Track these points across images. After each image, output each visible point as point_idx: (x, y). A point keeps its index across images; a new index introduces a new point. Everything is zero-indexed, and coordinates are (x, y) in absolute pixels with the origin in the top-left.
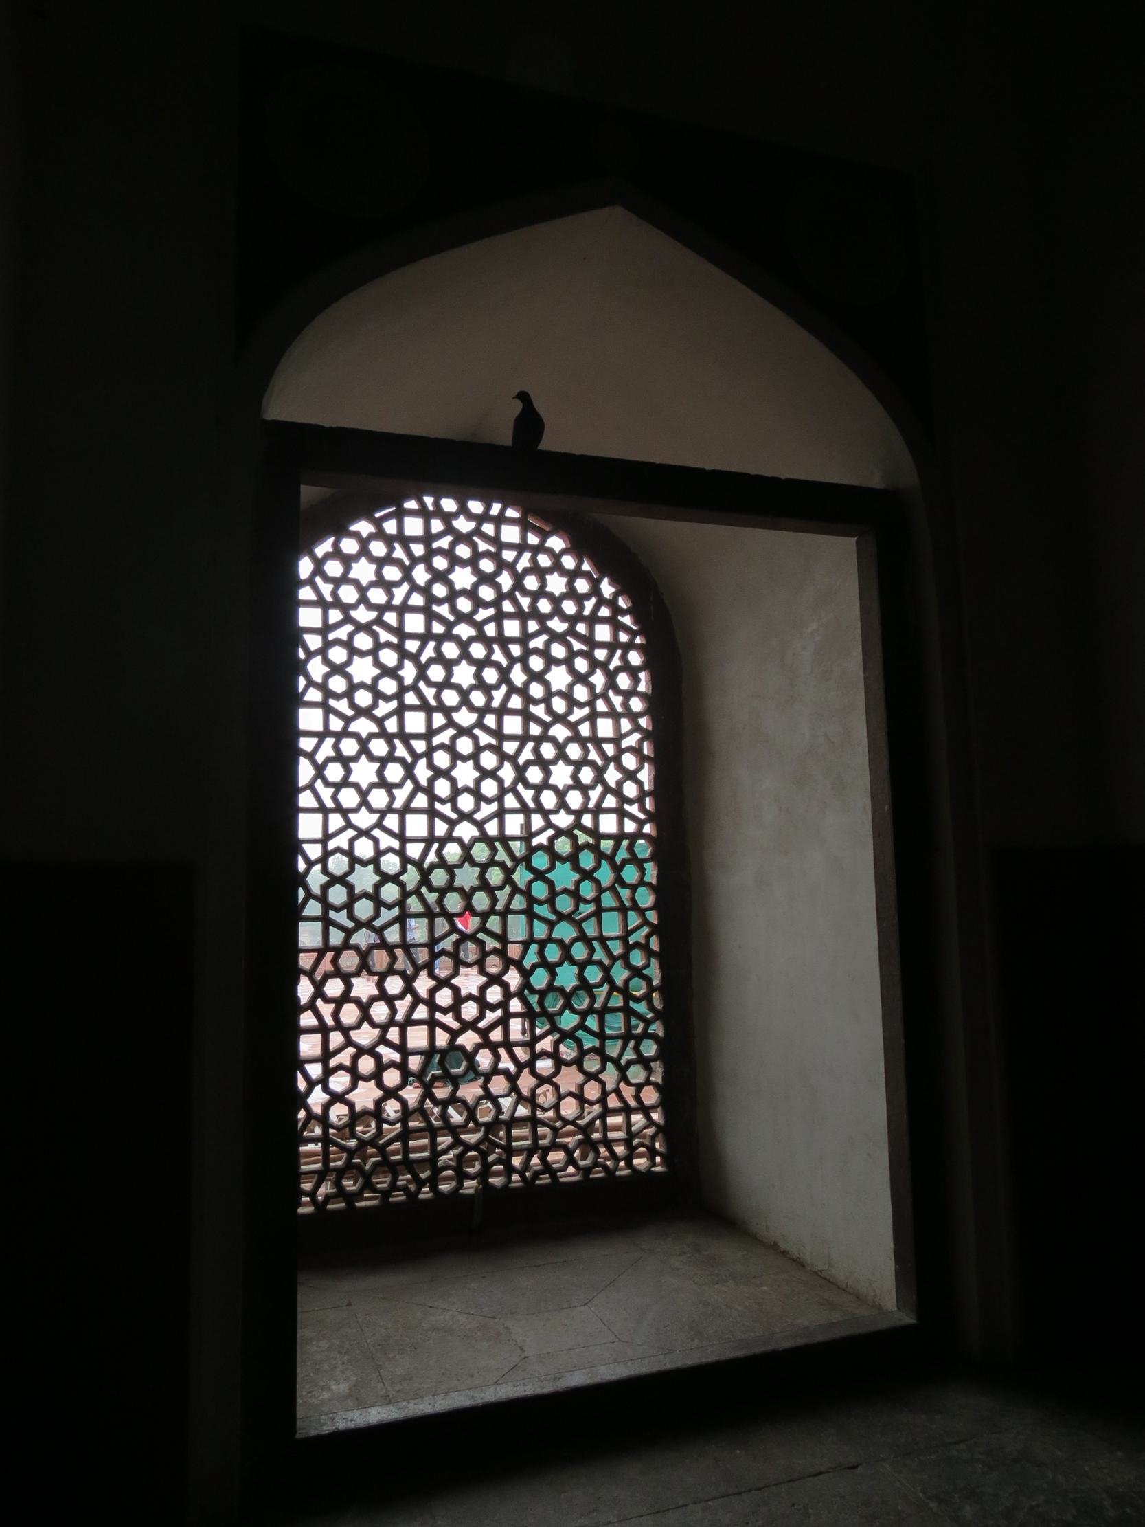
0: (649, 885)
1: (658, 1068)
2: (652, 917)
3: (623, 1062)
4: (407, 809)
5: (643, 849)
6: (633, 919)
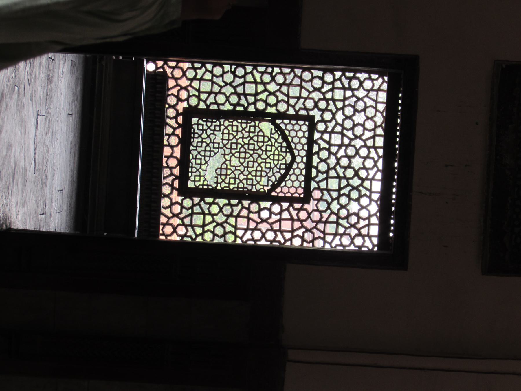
1: (222, 240)
4: (343, 135)
6: (288, 236)
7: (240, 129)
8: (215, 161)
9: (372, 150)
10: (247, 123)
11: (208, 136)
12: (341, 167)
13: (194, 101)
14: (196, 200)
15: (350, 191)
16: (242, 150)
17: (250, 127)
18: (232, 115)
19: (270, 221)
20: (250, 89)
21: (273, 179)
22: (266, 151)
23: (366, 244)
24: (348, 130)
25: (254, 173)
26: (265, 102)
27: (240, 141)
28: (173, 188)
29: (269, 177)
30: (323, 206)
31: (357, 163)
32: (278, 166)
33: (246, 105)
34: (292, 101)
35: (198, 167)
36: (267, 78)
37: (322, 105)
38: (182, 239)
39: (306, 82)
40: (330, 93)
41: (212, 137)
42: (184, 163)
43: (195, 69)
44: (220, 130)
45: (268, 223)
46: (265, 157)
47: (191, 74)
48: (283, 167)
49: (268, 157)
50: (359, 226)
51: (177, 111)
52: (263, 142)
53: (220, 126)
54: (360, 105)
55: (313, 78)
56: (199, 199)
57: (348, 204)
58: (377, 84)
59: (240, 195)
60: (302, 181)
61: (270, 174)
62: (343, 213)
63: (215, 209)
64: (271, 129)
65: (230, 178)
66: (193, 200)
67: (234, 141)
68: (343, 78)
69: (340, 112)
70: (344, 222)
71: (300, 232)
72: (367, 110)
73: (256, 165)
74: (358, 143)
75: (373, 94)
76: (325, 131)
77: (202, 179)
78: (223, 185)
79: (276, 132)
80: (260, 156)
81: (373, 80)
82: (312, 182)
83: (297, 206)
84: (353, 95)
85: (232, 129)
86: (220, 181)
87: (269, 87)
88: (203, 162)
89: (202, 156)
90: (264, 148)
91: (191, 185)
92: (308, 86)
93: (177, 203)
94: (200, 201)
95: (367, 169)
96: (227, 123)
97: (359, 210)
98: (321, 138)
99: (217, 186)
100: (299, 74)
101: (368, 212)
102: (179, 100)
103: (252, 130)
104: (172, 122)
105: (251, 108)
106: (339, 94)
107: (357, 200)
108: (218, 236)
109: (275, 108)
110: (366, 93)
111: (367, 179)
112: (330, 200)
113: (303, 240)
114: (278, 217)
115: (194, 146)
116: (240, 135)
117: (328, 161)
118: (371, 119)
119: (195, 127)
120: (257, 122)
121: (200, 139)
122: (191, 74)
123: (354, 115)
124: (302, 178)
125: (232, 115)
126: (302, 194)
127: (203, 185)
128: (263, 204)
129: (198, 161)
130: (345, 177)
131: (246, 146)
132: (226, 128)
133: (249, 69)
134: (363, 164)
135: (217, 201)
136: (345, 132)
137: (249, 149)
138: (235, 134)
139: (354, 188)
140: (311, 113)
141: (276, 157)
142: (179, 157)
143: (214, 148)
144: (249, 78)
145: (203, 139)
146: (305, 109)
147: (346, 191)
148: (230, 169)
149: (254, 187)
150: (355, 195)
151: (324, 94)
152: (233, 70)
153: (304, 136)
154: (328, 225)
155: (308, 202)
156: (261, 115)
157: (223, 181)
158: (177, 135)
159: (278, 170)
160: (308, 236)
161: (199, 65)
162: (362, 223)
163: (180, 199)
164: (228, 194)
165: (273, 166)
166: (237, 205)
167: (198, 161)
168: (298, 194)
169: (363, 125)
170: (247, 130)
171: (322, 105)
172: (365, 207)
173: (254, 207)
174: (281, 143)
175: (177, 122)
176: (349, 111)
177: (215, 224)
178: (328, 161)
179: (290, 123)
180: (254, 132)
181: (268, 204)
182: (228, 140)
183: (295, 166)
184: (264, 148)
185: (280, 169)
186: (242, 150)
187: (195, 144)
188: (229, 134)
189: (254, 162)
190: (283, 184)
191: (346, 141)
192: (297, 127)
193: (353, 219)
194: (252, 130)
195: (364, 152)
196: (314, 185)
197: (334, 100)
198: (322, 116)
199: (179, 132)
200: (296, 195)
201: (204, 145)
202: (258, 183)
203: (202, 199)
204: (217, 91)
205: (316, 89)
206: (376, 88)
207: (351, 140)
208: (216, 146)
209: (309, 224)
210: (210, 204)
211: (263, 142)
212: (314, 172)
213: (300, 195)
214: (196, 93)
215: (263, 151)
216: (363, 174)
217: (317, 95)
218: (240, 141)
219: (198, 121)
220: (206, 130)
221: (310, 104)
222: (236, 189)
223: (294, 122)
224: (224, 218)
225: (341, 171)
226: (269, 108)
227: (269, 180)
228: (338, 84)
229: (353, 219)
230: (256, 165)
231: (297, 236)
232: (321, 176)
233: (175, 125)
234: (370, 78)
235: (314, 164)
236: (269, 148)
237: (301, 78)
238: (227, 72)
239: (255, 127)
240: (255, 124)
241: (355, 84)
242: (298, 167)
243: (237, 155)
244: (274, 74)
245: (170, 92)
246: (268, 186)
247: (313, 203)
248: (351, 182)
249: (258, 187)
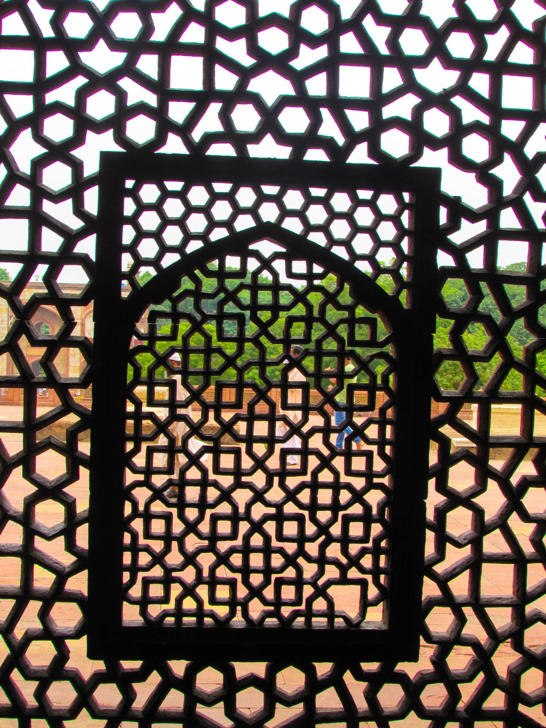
3: (514, 480)
14: (430, 589)
26: (53, 347)
28: (388, 675)
37: (59, 128)
51: (99, 678)
56: (426, 579)
65: (349, 472)
76: (159, 115)
80: (262, 364)
94: (434, 576)
98: (184, 131)
102: (58, 670)
115: (233, 613)
117: (270, 101)
124: (341, 201)
126: (399, 200)
128: (441, 340)
140: (91, 167)
143: (233, 536)
146: (75, 192)
153: (182, 195)
154: (507, 103)
163: (427, 651)
171: (59, 128)
175: (141, 675)
178: (270, 101)
179: (132, 249)
183: (293, 225)
187: (222, 611)
196: (360, 155)
199: (178, 667)
204: (19, 528)
212: (316, 155)
213: (402, 206)
214: (34, 607)
219: (133, 602)
220: (168, 570)
221: (57, 176)
222: (388, 449)
223: (128, 234)
226: (76, 333)
232: (329, 128)
233: (155, 678)
235: (284, 153)
242: (301, 214)
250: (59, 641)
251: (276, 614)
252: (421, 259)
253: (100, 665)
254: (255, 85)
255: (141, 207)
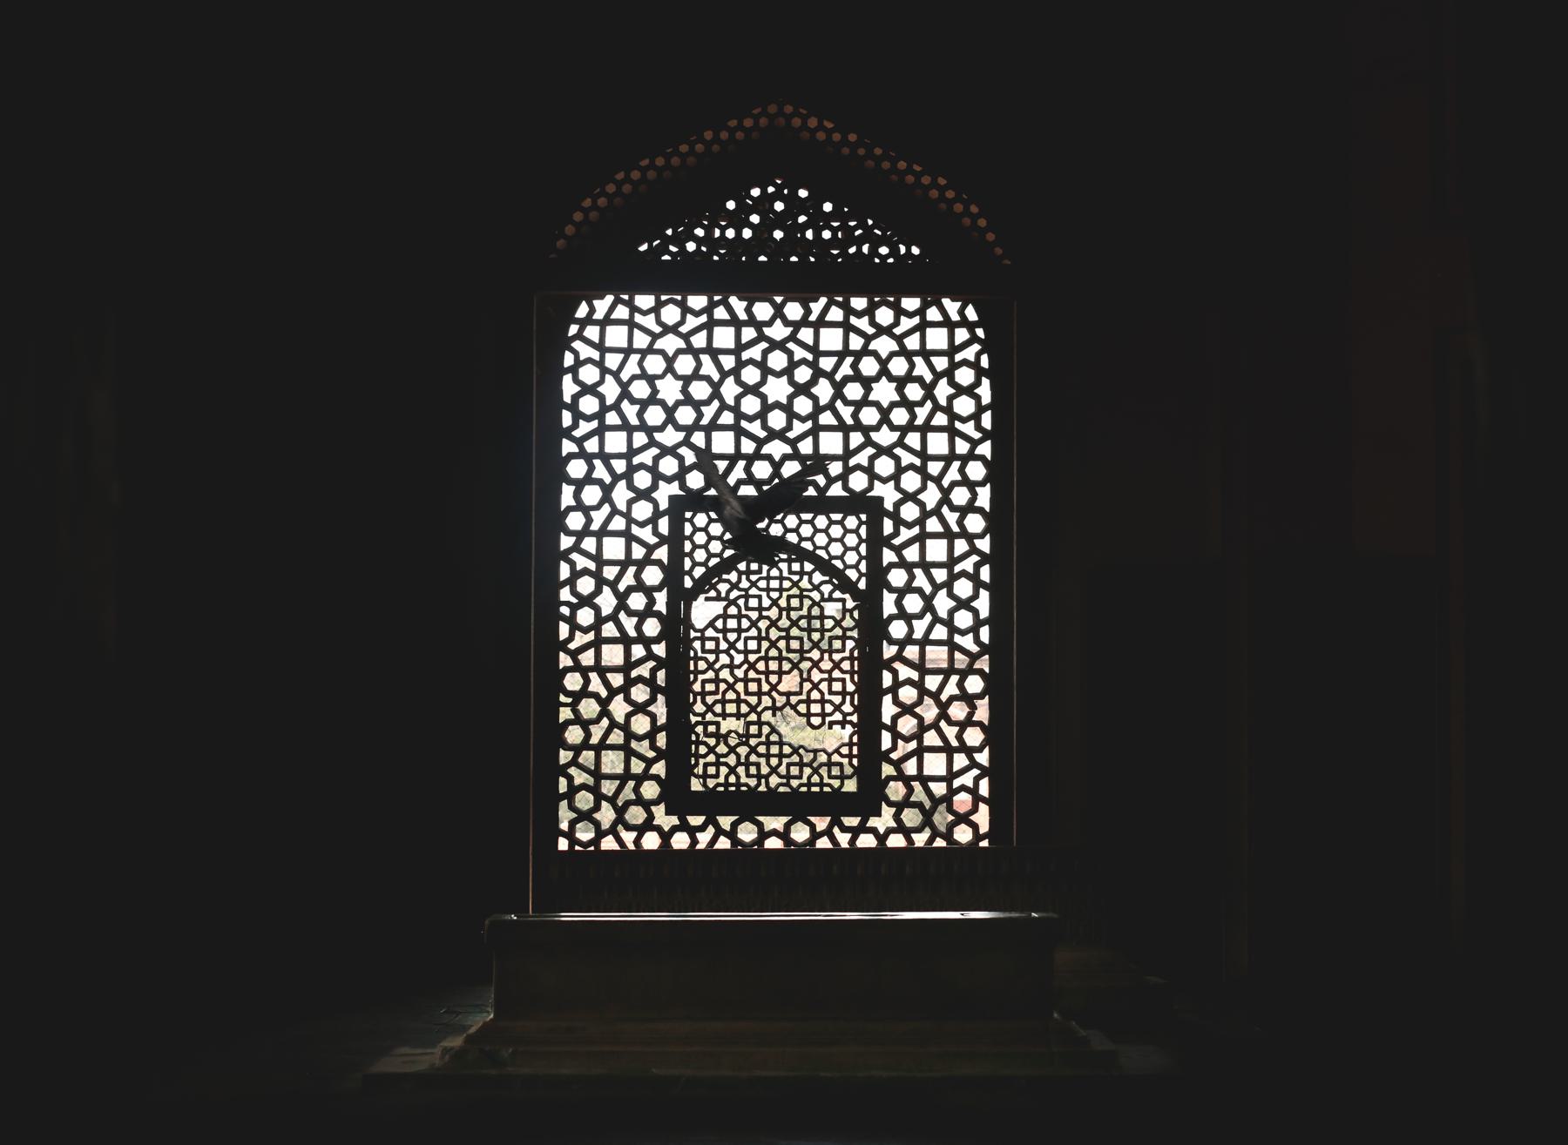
0: (980, 511)
2: (984, 545)
5: (976, 471)
7: (710, 675)
8: (793, 730)
9: (745, 355)
10: (696, 659)
11: (732, 750)
12: (789, 427)
13: (650, 790)
14: (887, 770)
15: (847, 403)
16: (761, 666)
17: (704, 651)
18: (678, 692)
19: (928, 589)
20: (613, 655)
21: (827, 589)
22: (760, 609)
23: (972, 358)
24: (700, 415)
25: (816, 636)
27: (739, 673)
29: (823, 599)
30: (885, 466)
31: (777, 389)
32: (795, 578)
33: (651, 664)
34: (638, 552)
35: (807, 771)
36: (585, 616)
37: (643, 480)
38: (984, 800)
39: (589, 521)
40: (614, 462)
41: (733, 741)
42: (798, 805)
43: (573, 790)
44: (718, 724)
45: (933, 595)
46: (775, 611)
47: (584, 800)
48: (796, 567)
49: (775, 603)
50: (928, 377)
51: (674, 829)
52: (739, 617)
53: (706, 724)
54: (640, 390)
55: (579, 506)
57: (877, 404)
58: (586, 352)
59: (870, 666)
60: (829, 518)
61: (816, 595)
62: (900, 416)
63: (907, 725)
64: (707, 599)
66: (890, 778)
67: (740, 687)
68: (577, 433)
69: (658, 436)
70: (922, 413)
71: (952, 518)
72: (650, 371)
73: (795, 632)
74: (730, 390)
75: (613, 361)
77: (835, 758)
78: (847, 708)
79: (713, 587)
81: (579, 363)
82: (830, 493)
83: (888, 526)
84: (616, 407)
85: (711, 693)
86: (838, 716)
87: (607, 610)
88: (795, 758)
89: (780, 764)
90: (754, 615)
91: (851, 786)
92: (598, 518)
93: (897, 817)
95: (793, 365)
96: (699, 707)
97: (891, 378)
99: (851, 722)
100: (572, 540)
101: (895, 359)
103: (710, 645)
104: (704, 839)
105: (660, 650)
106: (616, 442)
107: (867, 383)
108: (971, 714)
109: (656, 595)
110: (609, 378)
111: (813, 365)
112: (870, 451)
113: (970, 508)
114: (918, 572)
115: (759, 784)
116: (725, 674)
118: (670, 361)
119: (711, 783)
120: (693, 634)
121: (741, 770)
122: (584, 800)
123: (662, 403)
124: (821, 521)
125: (678, 692)
127: (850, 756)
128: (889, 607)
129: (795, 771)
130: (813, 416)
131: (752, 658)
132: (710, 708)
133: (565, 660)
134: (778, 375)
135: (886, 719)
136: (705, 421)
137: (758, 651)
138: (723, 686)
139: (838, 394)
140: (664, 505)
141: (775, 584)
142: (785, 819)
144: (587, 658)
145: (739, 763)
147: (846, 412)
148: (809, 692)
149: (849, 634)
150: (854, 391)
151: (616, 478)
152: (569, 700)
155: (880, 500)
156: (676, 626)
157: (838, 708)
158: (735, 825)
159: (806, 578)
160: (960, 496)
161: (563, 782)
162: (921, 368)
164: (869, 695)
165: (795, 591)
166: (895, 673)
167: (795, 771)
168: (859, 527)
169: (687, 380)
170: (711, 657)
171: (643, 480)
172: (884, 363)
173: (898, 629)
174: (740, 573)
176: (655, 416)
177: (943, 724)
179: (690, 555)
180: (716, 640)
181: (889, 601)
182: (738, 701)
184: (754, 615)
185: (802, 573)
186: (761, 666)
187: (753, 782)
188: (724, 702)
189: (788, 638)
190: (838, 564)
191: (727, 418)
192: (700, 538)
193: (914, 392)
194: (710, 645)
195: (751, 375)
197: (631, 452)
198: (669, 480)
200: (863, 531)
201: (753, 758)
202: (838, 623)
203: (885, 757)
205: (607, 498)
206: (596, 355)
207: (724, 407)
208: (754, 729)
209: (931, 497)
210: (896, 736)
211: (739, 617)
213: (861, 523)
215: (761, 617)
216: (803, 374)
217: (621, 494)
218: (739, 673)
219: (697, 776)
221: (642, 510)
223: (688, 546)
224: (928, 701)
225: (799, 428)
227: (830, 599)
228: (592, 446)
229: (914, 392)
230: (795, 632)
231: (960, 523)
234: (574, 370)
236: (753, 603)
237: (580, 535)
238: (575, 711)
239: (703, 639)
240: (696, 638)
241: (589, 405)
243: (774, 679)
244: (574, 600)
245: (631, 847)
246: (843, 601)
247: (879, 490)
248: (823, 401)
249: (848, 622)
250: (647, 805)
251: (787, 784)
252: (874, 557)
253: (674, 820)
254: (766, 450)
255: (696, 530)
